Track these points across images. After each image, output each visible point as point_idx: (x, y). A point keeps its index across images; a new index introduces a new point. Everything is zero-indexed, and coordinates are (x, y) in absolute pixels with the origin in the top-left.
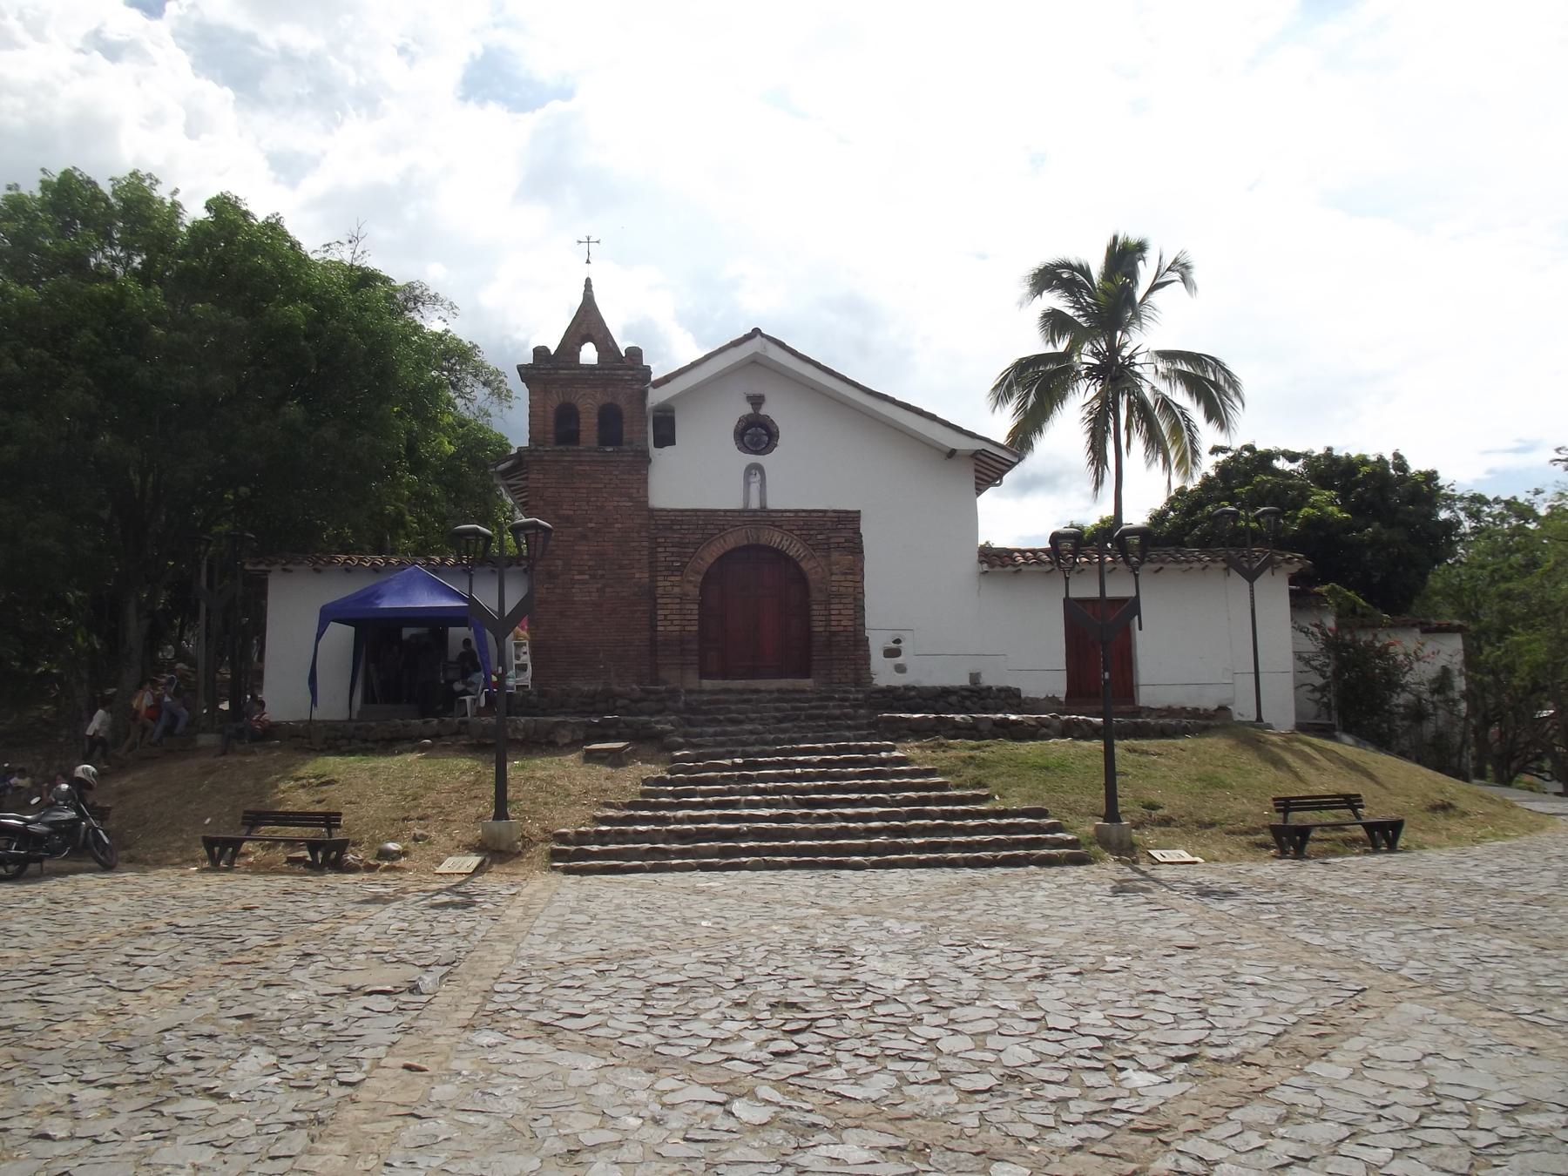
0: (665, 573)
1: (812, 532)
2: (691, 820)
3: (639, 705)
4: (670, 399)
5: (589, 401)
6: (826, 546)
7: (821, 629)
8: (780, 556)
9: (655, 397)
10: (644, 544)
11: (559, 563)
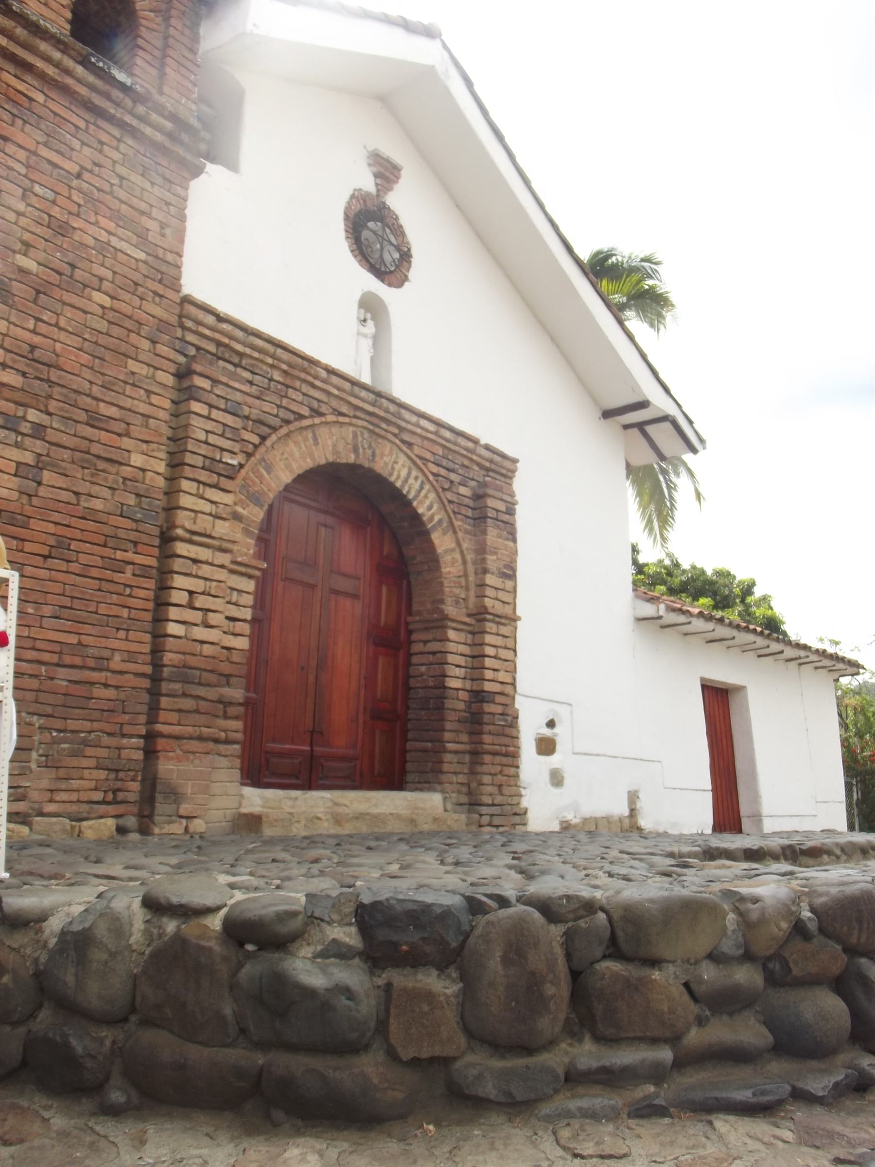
1: (453, 476)
6: (470, 513)
10: (162, 376)
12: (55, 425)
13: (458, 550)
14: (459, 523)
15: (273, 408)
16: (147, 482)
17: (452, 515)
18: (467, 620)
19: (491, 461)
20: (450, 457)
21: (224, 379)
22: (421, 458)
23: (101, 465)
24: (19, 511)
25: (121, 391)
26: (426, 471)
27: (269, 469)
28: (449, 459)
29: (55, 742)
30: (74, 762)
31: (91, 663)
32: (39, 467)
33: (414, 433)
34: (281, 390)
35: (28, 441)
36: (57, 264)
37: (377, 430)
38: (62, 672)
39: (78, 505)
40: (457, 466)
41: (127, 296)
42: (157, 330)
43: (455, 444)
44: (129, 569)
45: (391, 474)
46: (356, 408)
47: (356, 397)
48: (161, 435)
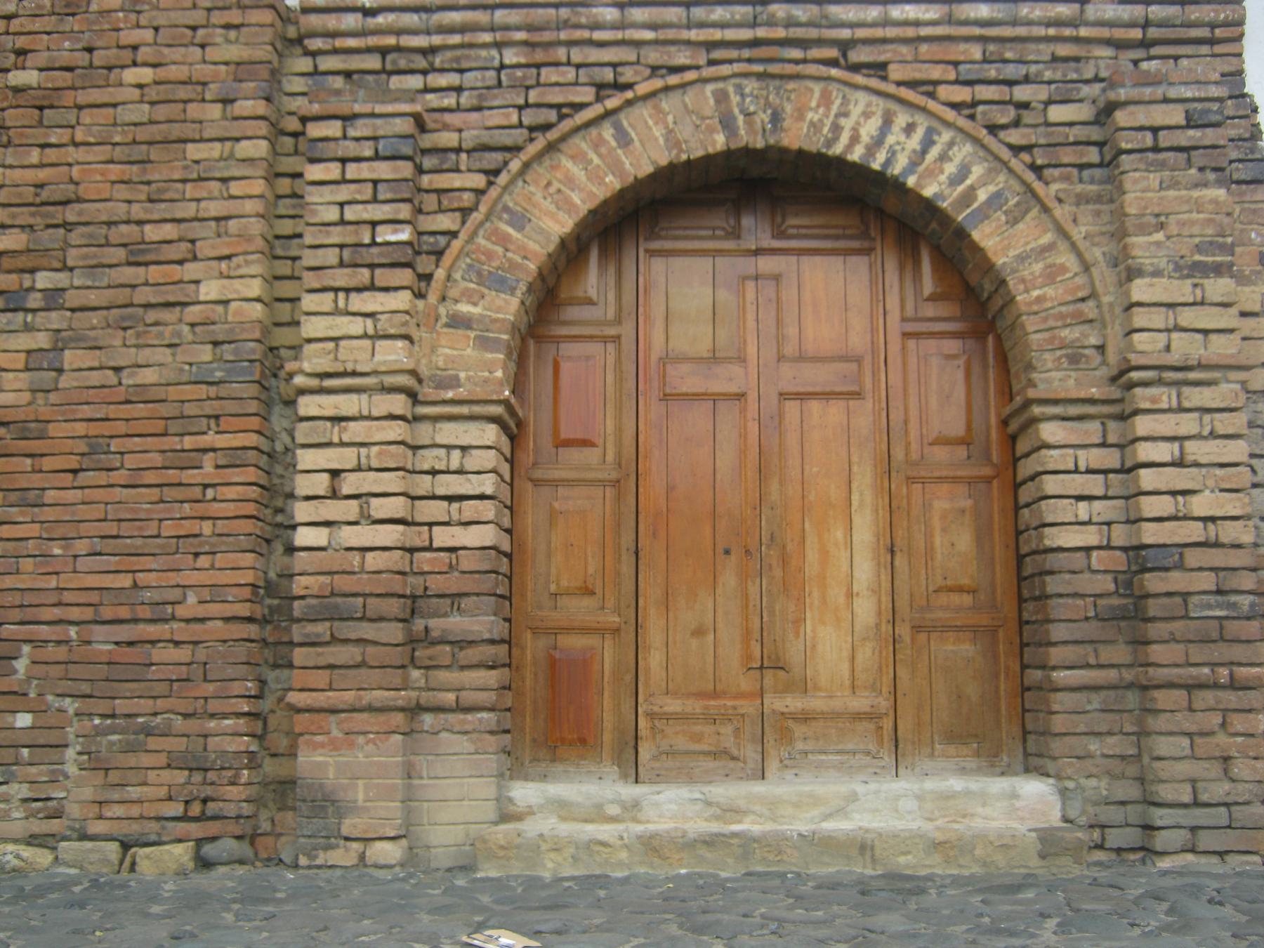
0: (341, 278)
1: (1021, 93)
6: (1093, 155)
7: (1090, 537)
10: (246, 149)
12: (77, 282)
13: (1063, 245)
14: (1054, 187)
15: (508, 116)
16: (230, 318)
17: (1030, 177)
18: (1094, 392)
19: (1146, 24)
20: (1009, 55)
21: (367, 108)
22: (912, 84)
23: (151, 316)
24: (32, 417)
25: (176, 196)
26: (932, 105)
27: (519, 221)
28: (1005, 61)
29: (101, 732)
30: (132, 760)
31: (145, 612)
32: (58, 349)
33: (884, 41)
34: (525, 77)
35: (40, 319)
36: (65, 58)
37: (774, 69)
38: (99, 632)
39: (120, 384)
40: (1033, 69)
41: (177, 54)
42: (235, 80)
43: (1014, 23)
44: (208, 460)
45: (830, 143)
46: (710, 45)
47: (702, 25)
48: (250, 239)
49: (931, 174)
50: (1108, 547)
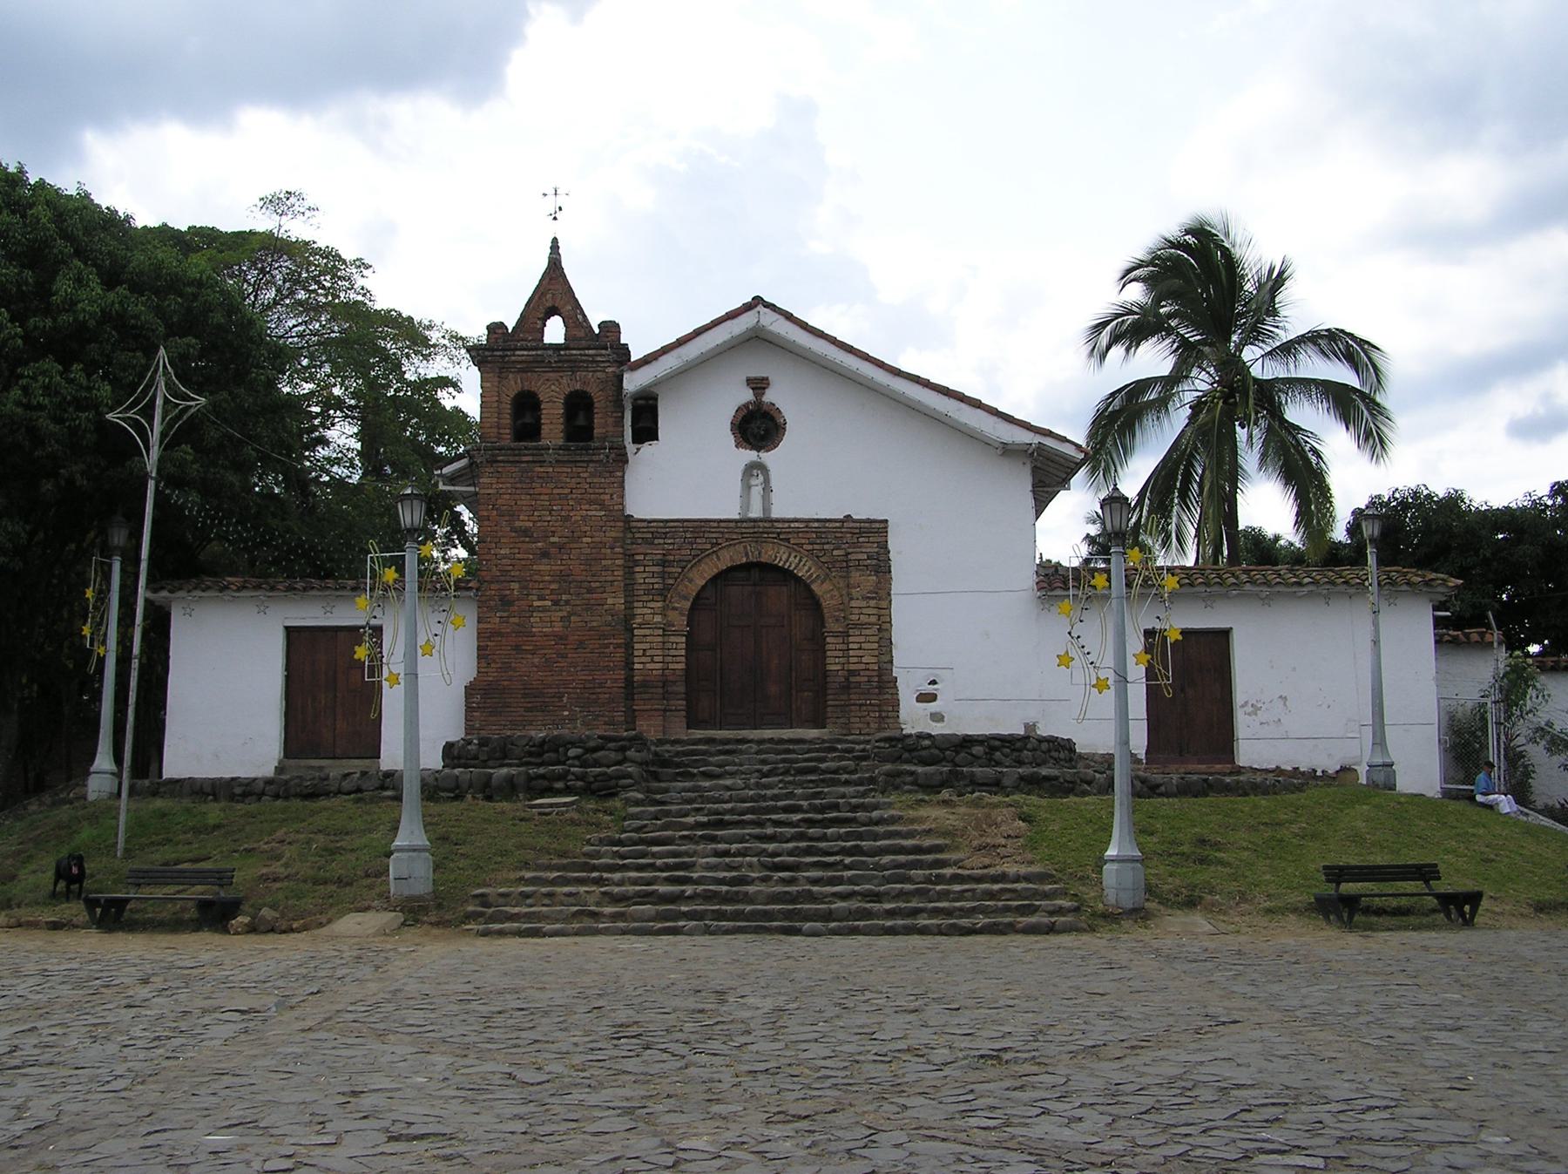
0: (645, 598)
1: (826, 547)
2: (635, 882)
3: (595, 755)
4: (650, 385)
5: (553, 387)
6: (845, 564)
7: (839, 667)
8: (785, 575)
9: (633, 382)
11: (515, 586)
27: (691, 581)
36: (567, 534)
44: (611, 647)
49: (800, 570)
50: (843, 670)
